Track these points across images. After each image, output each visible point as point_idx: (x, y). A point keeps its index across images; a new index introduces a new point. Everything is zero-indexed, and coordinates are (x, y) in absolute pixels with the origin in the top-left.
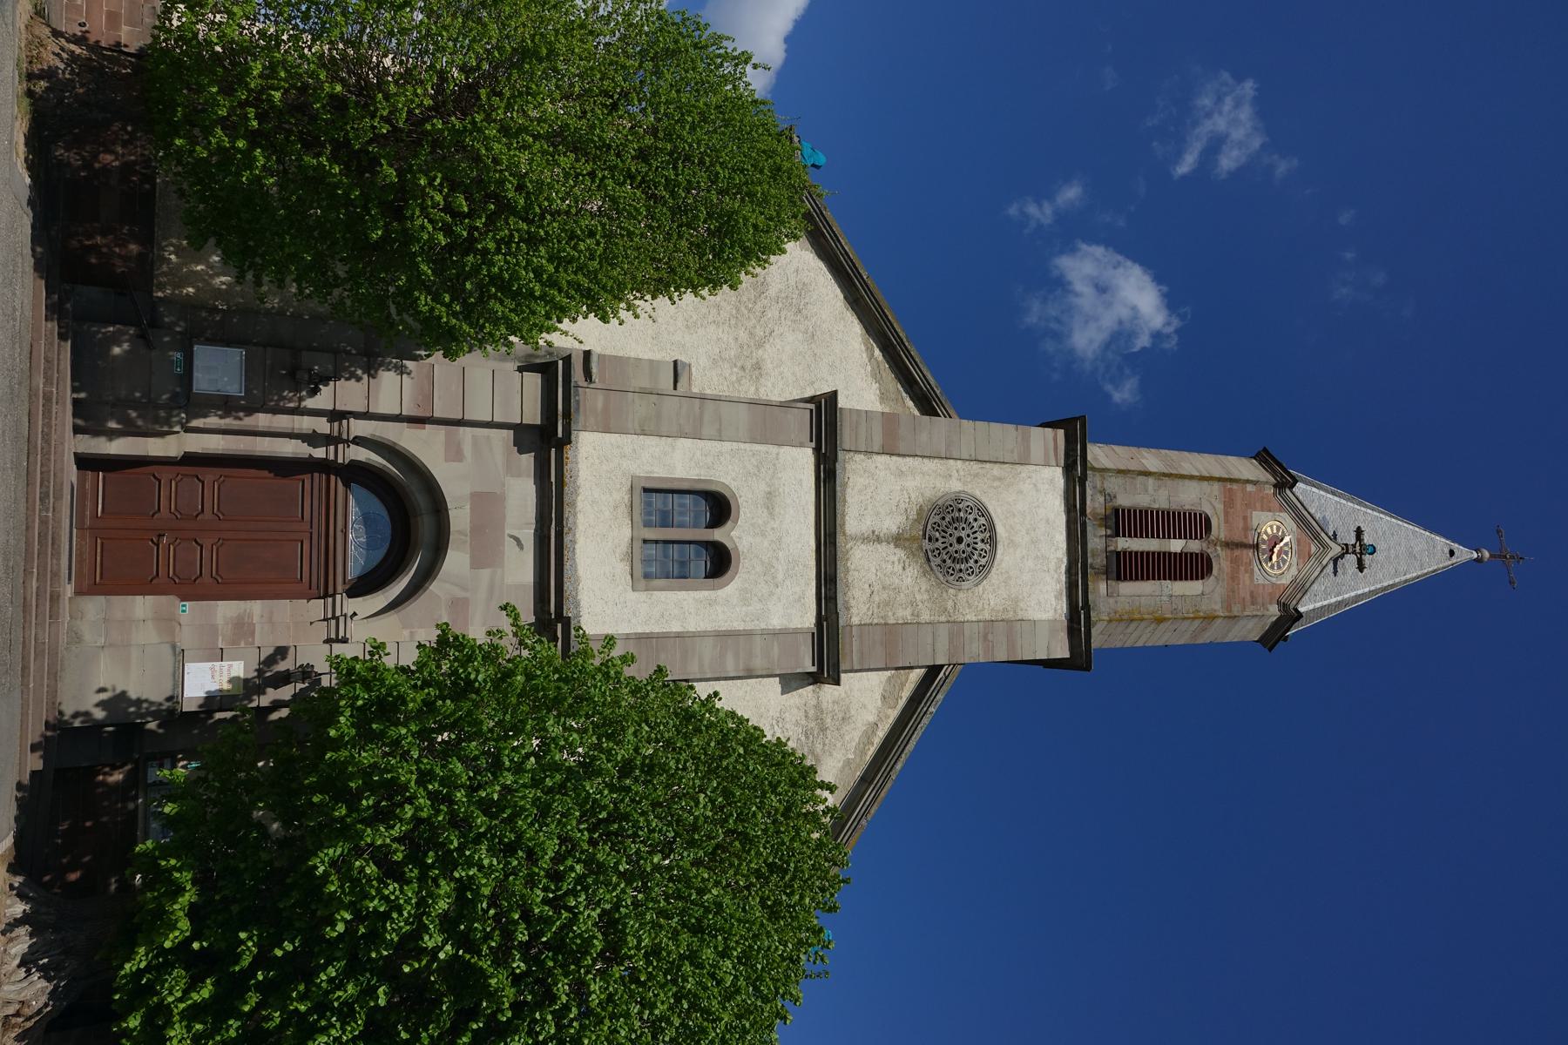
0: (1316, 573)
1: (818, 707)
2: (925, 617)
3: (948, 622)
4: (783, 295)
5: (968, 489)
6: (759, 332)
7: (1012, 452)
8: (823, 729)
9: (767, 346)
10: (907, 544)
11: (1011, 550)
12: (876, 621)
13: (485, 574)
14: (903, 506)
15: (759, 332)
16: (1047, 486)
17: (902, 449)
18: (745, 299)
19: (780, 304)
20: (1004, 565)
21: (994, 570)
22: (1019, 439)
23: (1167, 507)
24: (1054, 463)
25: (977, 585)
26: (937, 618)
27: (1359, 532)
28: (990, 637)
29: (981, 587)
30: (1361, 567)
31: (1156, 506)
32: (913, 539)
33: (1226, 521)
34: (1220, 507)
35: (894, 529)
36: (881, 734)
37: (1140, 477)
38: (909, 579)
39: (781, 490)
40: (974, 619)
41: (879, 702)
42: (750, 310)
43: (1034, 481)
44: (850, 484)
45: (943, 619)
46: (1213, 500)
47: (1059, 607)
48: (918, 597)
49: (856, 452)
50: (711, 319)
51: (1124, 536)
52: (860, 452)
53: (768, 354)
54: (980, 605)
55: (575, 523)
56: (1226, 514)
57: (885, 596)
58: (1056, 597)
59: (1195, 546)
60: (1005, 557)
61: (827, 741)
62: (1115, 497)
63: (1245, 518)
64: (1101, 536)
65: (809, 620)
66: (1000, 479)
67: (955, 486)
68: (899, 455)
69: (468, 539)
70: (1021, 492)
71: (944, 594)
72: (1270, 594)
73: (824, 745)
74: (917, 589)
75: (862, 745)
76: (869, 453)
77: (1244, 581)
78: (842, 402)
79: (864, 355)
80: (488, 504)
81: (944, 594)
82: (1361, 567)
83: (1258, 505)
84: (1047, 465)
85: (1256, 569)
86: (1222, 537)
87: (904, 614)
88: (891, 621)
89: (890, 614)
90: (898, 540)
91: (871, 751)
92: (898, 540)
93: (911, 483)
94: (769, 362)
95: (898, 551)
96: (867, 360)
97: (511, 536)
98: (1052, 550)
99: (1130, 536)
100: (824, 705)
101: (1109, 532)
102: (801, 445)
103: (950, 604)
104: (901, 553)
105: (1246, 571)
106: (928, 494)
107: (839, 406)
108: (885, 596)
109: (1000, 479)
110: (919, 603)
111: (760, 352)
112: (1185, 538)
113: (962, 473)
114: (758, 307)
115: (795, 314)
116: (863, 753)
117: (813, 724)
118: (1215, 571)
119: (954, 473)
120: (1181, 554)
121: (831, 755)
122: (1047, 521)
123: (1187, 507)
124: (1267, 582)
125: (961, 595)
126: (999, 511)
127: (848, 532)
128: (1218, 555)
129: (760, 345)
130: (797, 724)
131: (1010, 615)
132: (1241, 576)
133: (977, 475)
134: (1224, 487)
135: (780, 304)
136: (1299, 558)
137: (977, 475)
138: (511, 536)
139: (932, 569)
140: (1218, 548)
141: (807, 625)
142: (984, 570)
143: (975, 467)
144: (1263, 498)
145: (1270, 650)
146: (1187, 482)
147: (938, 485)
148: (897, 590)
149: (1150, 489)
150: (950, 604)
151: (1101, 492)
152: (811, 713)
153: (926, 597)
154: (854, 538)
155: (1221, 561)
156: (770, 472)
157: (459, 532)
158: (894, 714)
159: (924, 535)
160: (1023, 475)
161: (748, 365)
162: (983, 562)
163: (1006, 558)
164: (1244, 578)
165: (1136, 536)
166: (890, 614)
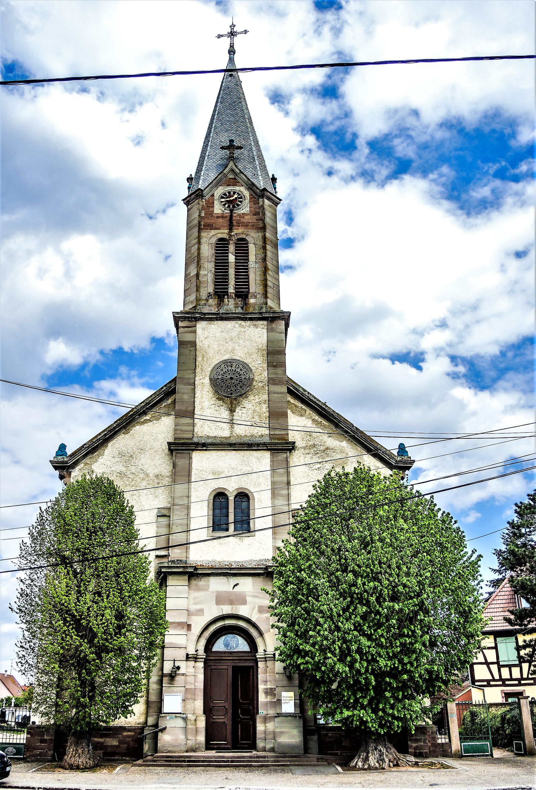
0: (244, 177)
1: (305, 448)
2: (266, 397)
3: (268, 385)
4: (125, 464)
5: (208, 374)
6: (142, 476)
7: (190, 351)
8: (314, 446)
9: (148, 472)
10: (234, 406)
11: (235, 352)
12: (268, 422)
13: (249, 599)
14: (217, 408)
15: (142, 476)
16: (206, 332)
17: (192, 408)
18: (128, 483)
19: (129, 465)
20: (242, 356)
21: (245, 361)
22: (184, 346)
23: (213, 263)
24: (195, 328)
25: (251, 370)
26: (267, 391)
27: (223, 148)
28: (275, 364)
29: (253, 368)
30: (240, 148)
31: (213, 270)
32: (231, 403)
33: (219, 229)
34: (213, 232)
35: (227, 412)
36: (317, 417)
37: (200, 279)
38: (250, 405)
39: (211, 468)
40: (267, 372)
41: (304, 418)
42: (133, 480)
43: (203, 339)
44: (208, 434)
45: (267, 388)
46: (209, 236)
47: (261, 327)
48: (257, 400)
49: (193, 431)
50: (137, 499)
51: (227, 289)
52: (194, 429)
53: (152, 472)
54: (260, 368)
55: (227, 562)
56: (216, 229)
57: (257, 417)
58: (257, 328)
59: (232, 248)
60: (240, 355)
61: (320, 444)
62: (209, 293)
63: (218, 217)
64: (228, 301)
65: (267, 455)
66: (203, 357)
67: (207, 381)
68: (194, 410)
69: (235, 606)
70: (209, 346)
71: (256, 387)
72: (254, 204)
73: (321, 445)
74: (253, 401)
75: (322, 427)
76: (194, 425)
77: (248, 219)
78: (171, 440)
79: (149, 424)
80: (220, 599)
81: (256, 387)
82: (240, 148)
83: (211, 209)
84: (195, 332)
85: (242, 212)
86: (227, 231)
87: (264, 408)
88: (267, 414)
89: (264, 415)
90: (232, 411)
91: (324, 422)
92: (232, 411)
93: (206, 404)
94: (155, 471)
95: (237, 410)
96: (151, 423)
97: (233, 588)
98: (235, 329)
99: (228, 285)
100: (304, 445)
101: (226, 297)
102: (191, 458)
103: (260, 385)
104: (237, 410)
105: (244, 217)
106: (211, 395)
107: (173, 441)
108: (257, 417)
109: (203, 357)
110: (260, 400)
111: (150, 475)
112: (228, 253)
113: (201, 377)
114: (131, 476)
115: (133, 458)
116: (325, 426)
117: (312, 450)
118: (244, 236)
119: (202, 381)
120: (236, 256)
121: (325, 442)
122: (222, 332)
123: (213, 252)
124: (249, 205)
125: (256, 379)
126: (217, 358)
127: (229, 435)
128: (236, 234)
129: (147, 475)
130: (311, 458)
131: (265, 353)
132: (246, 221)
133: (202, 369)
134: (203, 229)
135: (129, 465)
136: (236, 185)
137: (202, 369)
138: (233, 588)
139: (245, 393)
140: (232, 234)
141: (269, 456)
142: (245, 366)
143: (198, 370)
144: (207, 207)
145: (280, 200)
146: (201, 251)
147: (207, 390)
148: (254, 411)
149: (206, 273)
150: (260, 385)
151: (207, 301)
152: (307, 451)
153: (257, 397)
154: (232, 432)
155: (238, 231)
156: (204, 473)
157: (232, 610)
158: (309, 411)
159: (229, 397)
160: (201, 345)
161: (157, 481)
162: (241, 366)
163: (239, 354)
164: (247, 219)
165: (227, 282)
166: (264, 415)
